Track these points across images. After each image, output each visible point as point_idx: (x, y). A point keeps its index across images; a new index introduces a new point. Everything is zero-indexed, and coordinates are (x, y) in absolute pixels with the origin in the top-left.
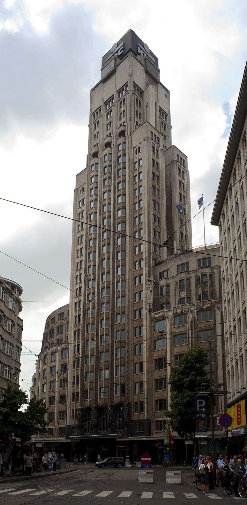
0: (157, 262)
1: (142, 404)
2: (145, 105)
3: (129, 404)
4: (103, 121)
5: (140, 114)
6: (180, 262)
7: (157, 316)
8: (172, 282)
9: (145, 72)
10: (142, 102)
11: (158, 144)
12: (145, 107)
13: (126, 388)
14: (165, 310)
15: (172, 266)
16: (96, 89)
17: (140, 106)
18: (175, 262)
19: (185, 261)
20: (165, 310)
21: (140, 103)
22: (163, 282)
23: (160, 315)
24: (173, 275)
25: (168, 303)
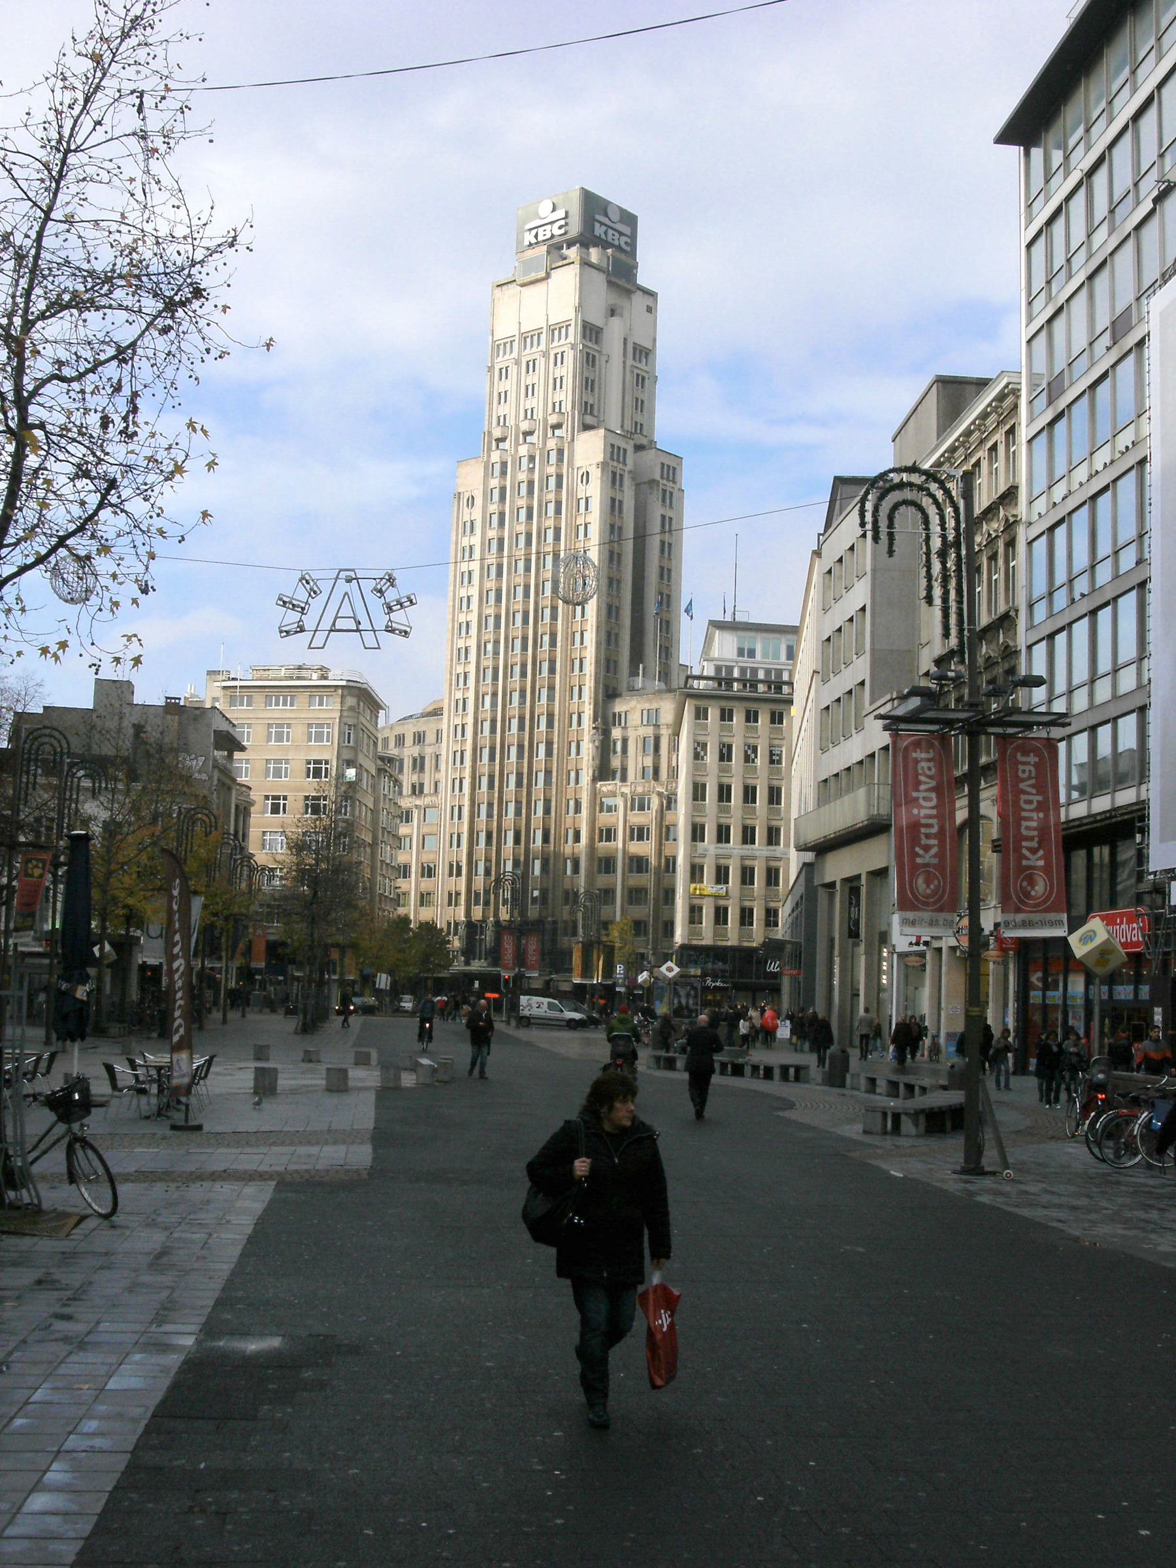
0: (610, 692)
1: (575, 923)
2: (604, 358)
3: (555, 922)
4: (519, 374)
5: (593, 381)
6: (647, 706)
7: (604, 789)
8: (632, 735)
9: (605, 284)
10: (597, 355)
11: (625, 464)
12: (603, 363)
13: (550, 896)
14: (617, 781)
15: (633, 709)
16: (505, 287)
17: (593, 366)
18: (638, 702)
19: (654, 706)
20: (619, 784)
21: (594, 357)
22: (616, 733)
23: (610, 788)
24: (634, 723)
25: (624, 770)
